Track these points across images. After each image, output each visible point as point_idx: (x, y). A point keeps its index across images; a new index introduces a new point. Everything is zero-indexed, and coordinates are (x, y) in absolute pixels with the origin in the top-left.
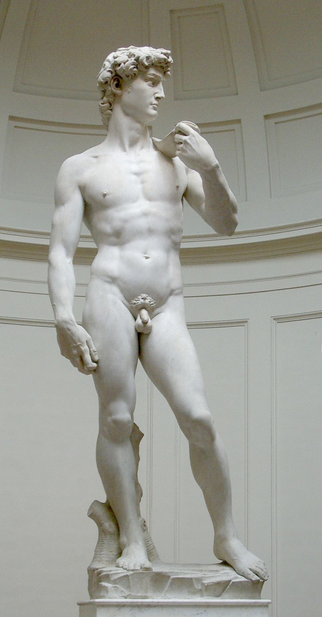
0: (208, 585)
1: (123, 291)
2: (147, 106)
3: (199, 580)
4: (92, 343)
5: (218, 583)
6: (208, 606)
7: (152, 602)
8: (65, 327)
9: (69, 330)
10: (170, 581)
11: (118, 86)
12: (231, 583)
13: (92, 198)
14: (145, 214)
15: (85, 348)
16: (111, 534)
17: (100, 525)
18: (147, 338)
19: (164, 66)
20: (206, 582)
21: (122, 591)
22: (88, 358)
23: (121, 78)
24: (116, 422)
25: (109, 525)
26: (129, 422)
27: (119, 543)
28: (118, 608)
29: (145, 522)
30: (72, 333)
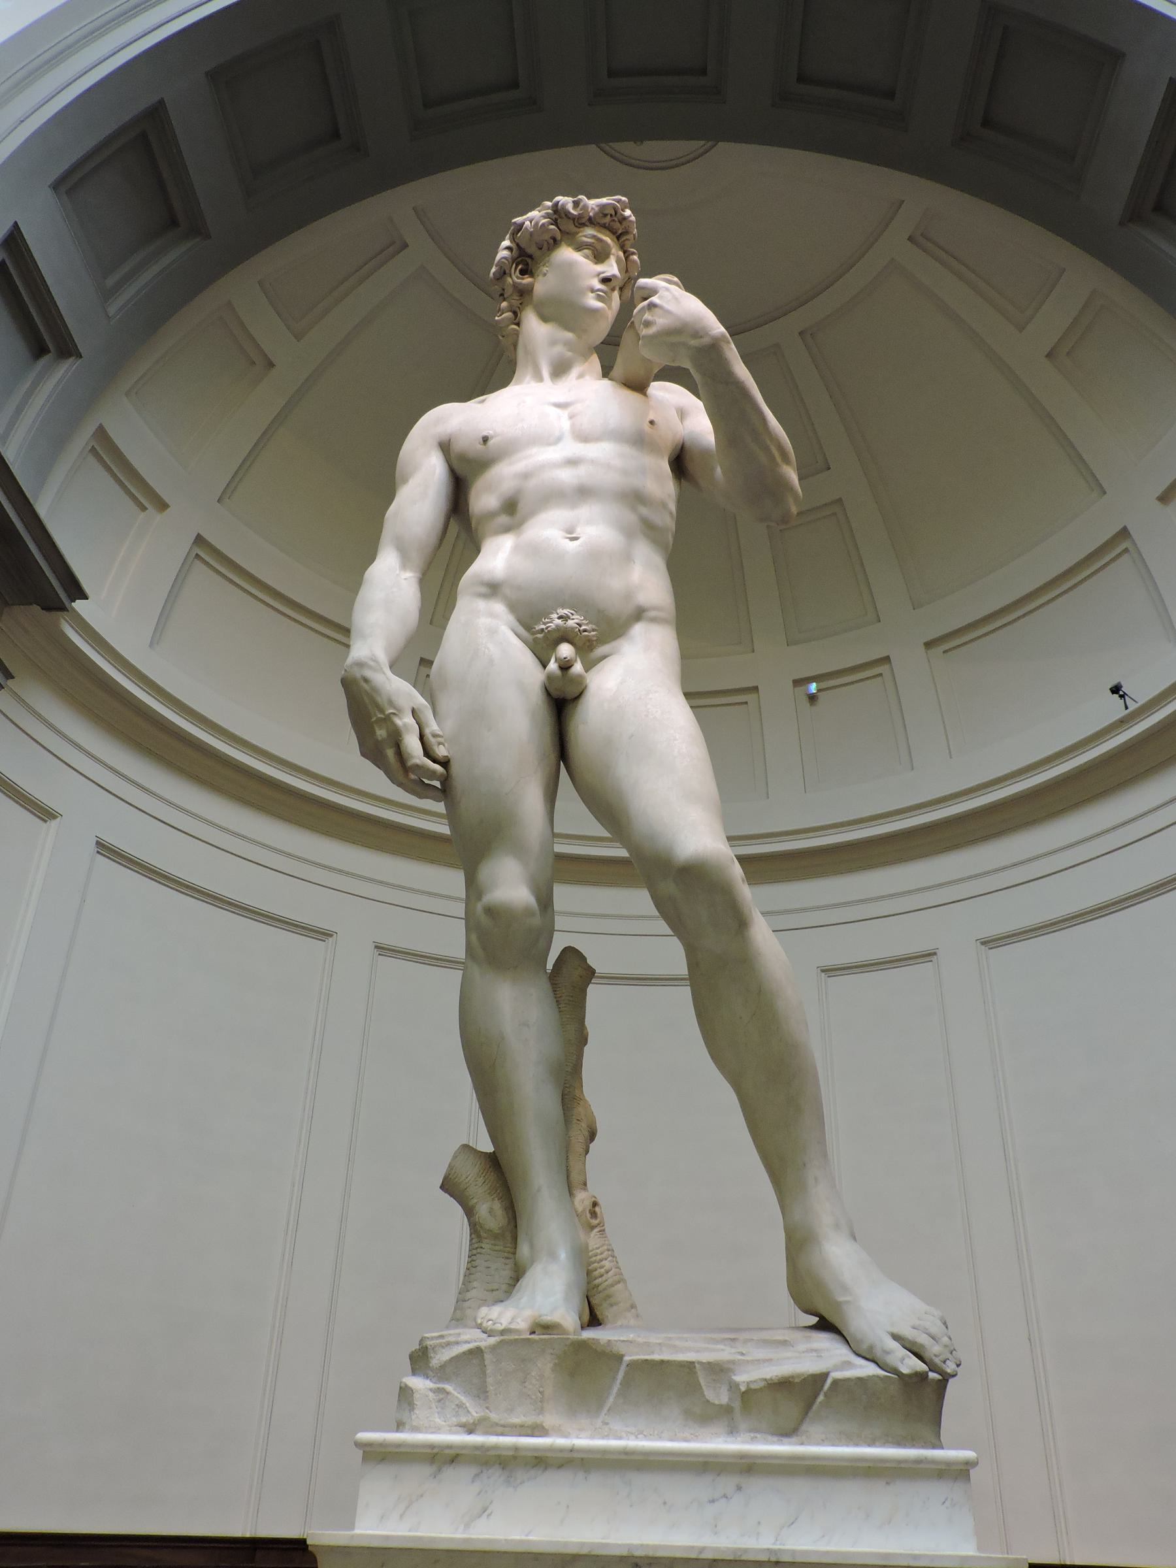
1: (513, 607)
2: (582, 292)
3: (718, 1370)
5: (784, 1385)
6: (749, 1467)
7: (551, 1449)
8: (358, 675)
9: (366, 680)
10: (623, 1368)
11: (523, 272)
13: (464, 458)
14: (572, 462)
15: (406, 721)
16: (496, 1237)
17: (469, 1212)
19: (617, 225)
20: (743, 1378)
21: (460, 1406)
22: (412, 744)
23: (531, 257)
24: (490, 911)
25: (490, 1211)
26: (528, 912)
28: (427, 1470)
29: (595, 1204)
30: (375, 690)
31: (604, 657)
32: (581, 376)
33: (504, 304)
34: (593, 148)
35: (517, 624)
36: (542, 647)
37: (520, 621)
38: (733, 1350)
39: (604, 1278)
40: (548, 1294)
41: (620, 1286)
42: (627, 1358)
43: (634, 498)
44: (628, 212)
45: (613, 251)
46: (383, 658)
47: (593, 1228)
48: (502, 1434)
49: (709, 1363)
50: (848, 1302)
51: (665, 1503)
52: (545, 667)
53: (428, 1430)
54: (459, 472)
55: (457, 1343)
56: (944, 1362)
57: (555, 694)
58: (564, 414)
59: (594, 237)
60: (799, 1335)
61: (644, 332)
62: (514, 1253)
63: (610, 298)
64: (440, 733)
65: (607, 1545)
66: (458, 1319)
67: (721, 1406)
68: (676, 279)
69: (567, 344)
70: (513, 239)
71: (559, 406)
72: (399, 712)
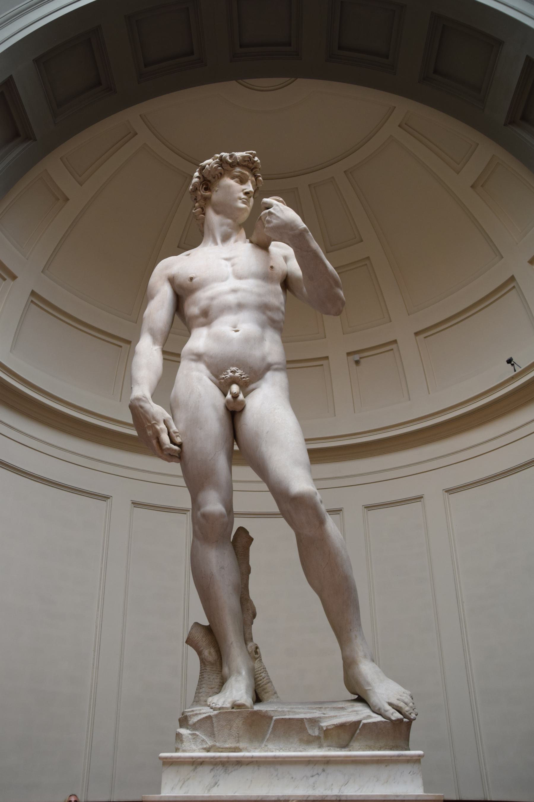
0: (327, 730)
1: (209, 366)
3: (314, 722)
4: (172, 423)
5: (342, 726)
6: (327, 762)
7: (243, 757)
9: (142, 407)
10: (273, 722)
11: (207, 189)
12: (361, 724)
14: (234, 291)
16: (212, 664)
17: (200, 653)
18: (241, 416)
19: (251, 165)
20: (324, 724)
22: (165, 438)
23: (209, 181)
25: (209, 653)
26: (221, 515)
27: (222, 676)
29: (257, 648)
30: (146, 412)
31: (253, 390)
32: (236, 241)
33: (197, 204)
34: (234, 82)
35: (211, 375)
36: (224, 387)
37: (212, 373)
38: (320, 712)
39: (262, 681)
40: (238, 691)
41: (269, 684)
42: (274, 718)
43: (264, 308)
44: (256, 159)
45: (250, 178)
46: (148, 395)
47: (256, 659)
48: (222, 752)
49: (310, 719)
50: (370, 690)
51: (292, 778)
52: (225, 395)
53: (189, 751)
54: (179, 293)
55: (200, 714)
56: (410, 714)
57: (230, 409)
58: (228, 263)
59: (240, 172)
60: (349, 704)
61: (266, 226)
62: (221, 671)
63: (249, 202)
64: (177, 431)
65: (268, 796)
66: (197, 701)
67: (315, 736)
68: (281, 199)
69: (228, 225)
70: (200, 172)
71: (227, 259)
72: (158, 422)
